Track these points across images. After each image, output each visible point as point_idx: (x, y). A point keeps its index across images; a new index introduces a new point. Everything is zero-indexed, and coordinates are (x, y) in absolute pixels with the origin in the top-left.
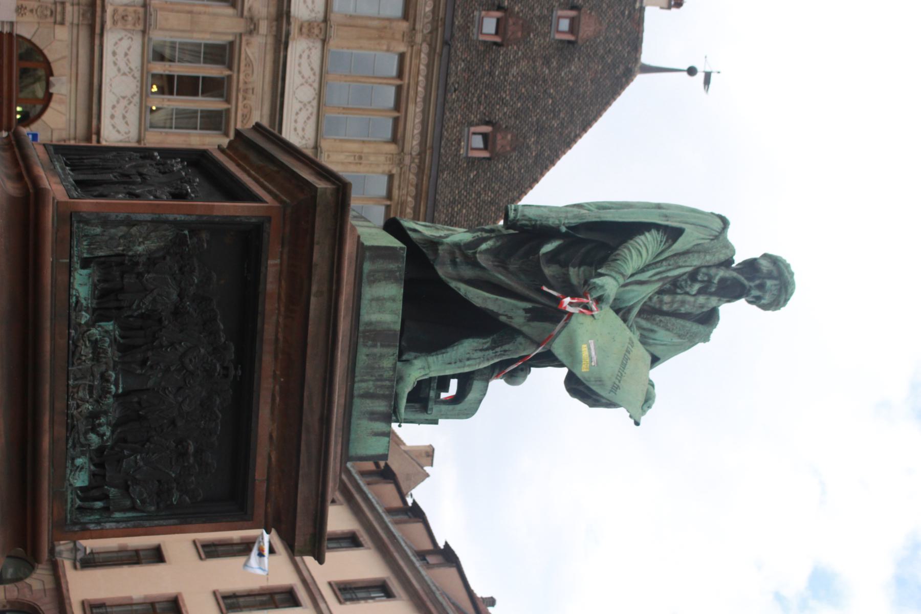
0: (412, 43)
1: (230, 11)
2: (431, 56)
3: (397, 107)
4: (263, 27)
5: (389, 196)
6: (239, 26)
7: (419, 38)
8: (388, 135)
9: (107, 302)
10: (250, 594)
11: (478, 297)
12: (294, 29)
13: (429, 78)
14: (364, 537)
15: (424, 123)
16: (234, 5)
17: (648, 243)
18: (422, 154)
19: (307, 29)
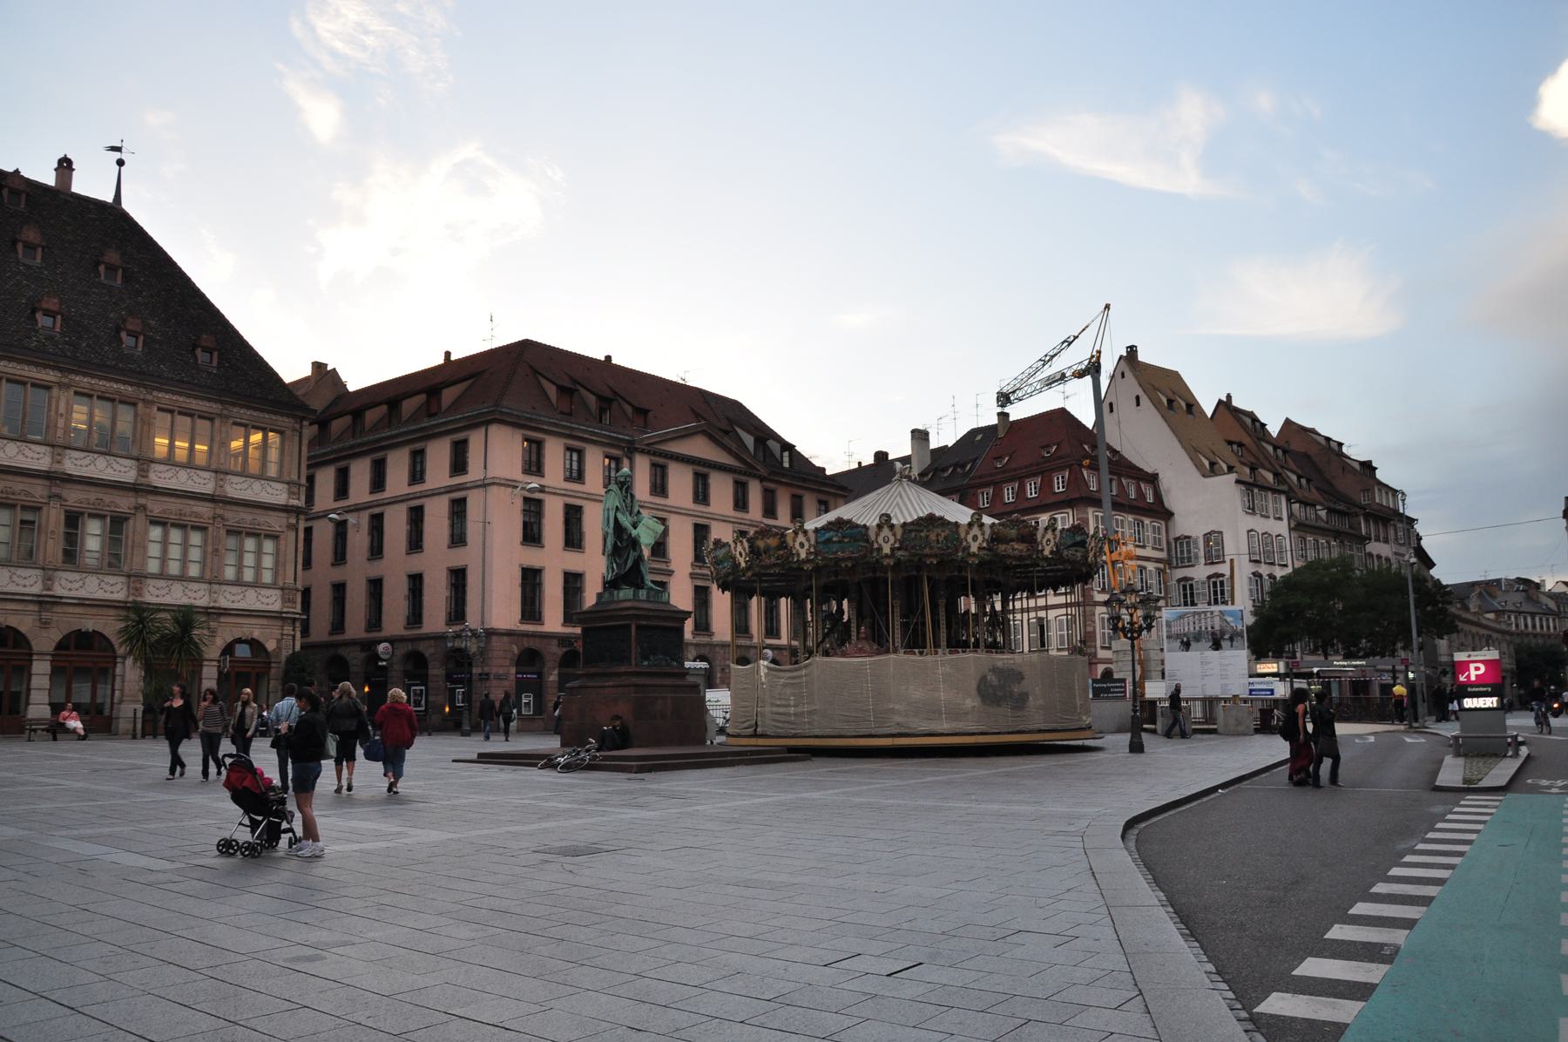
0: (153, 402)
1: (131, 522)
2: (160, 390)
3: (191, 415)
4: (142, 501)
5: (245, 426)
6: (141, 517)
7: (149, 397)
8: (208, 423)
9: (646, 658)
10: (452, 526)
11: (630, 563)
12: (143, 481)
13: (174, 393)
14: (418, 446)
15: (202, 399)
16: (127, 519)
17: (620, 516)
18: (222, 402)
19: (143, 472)
